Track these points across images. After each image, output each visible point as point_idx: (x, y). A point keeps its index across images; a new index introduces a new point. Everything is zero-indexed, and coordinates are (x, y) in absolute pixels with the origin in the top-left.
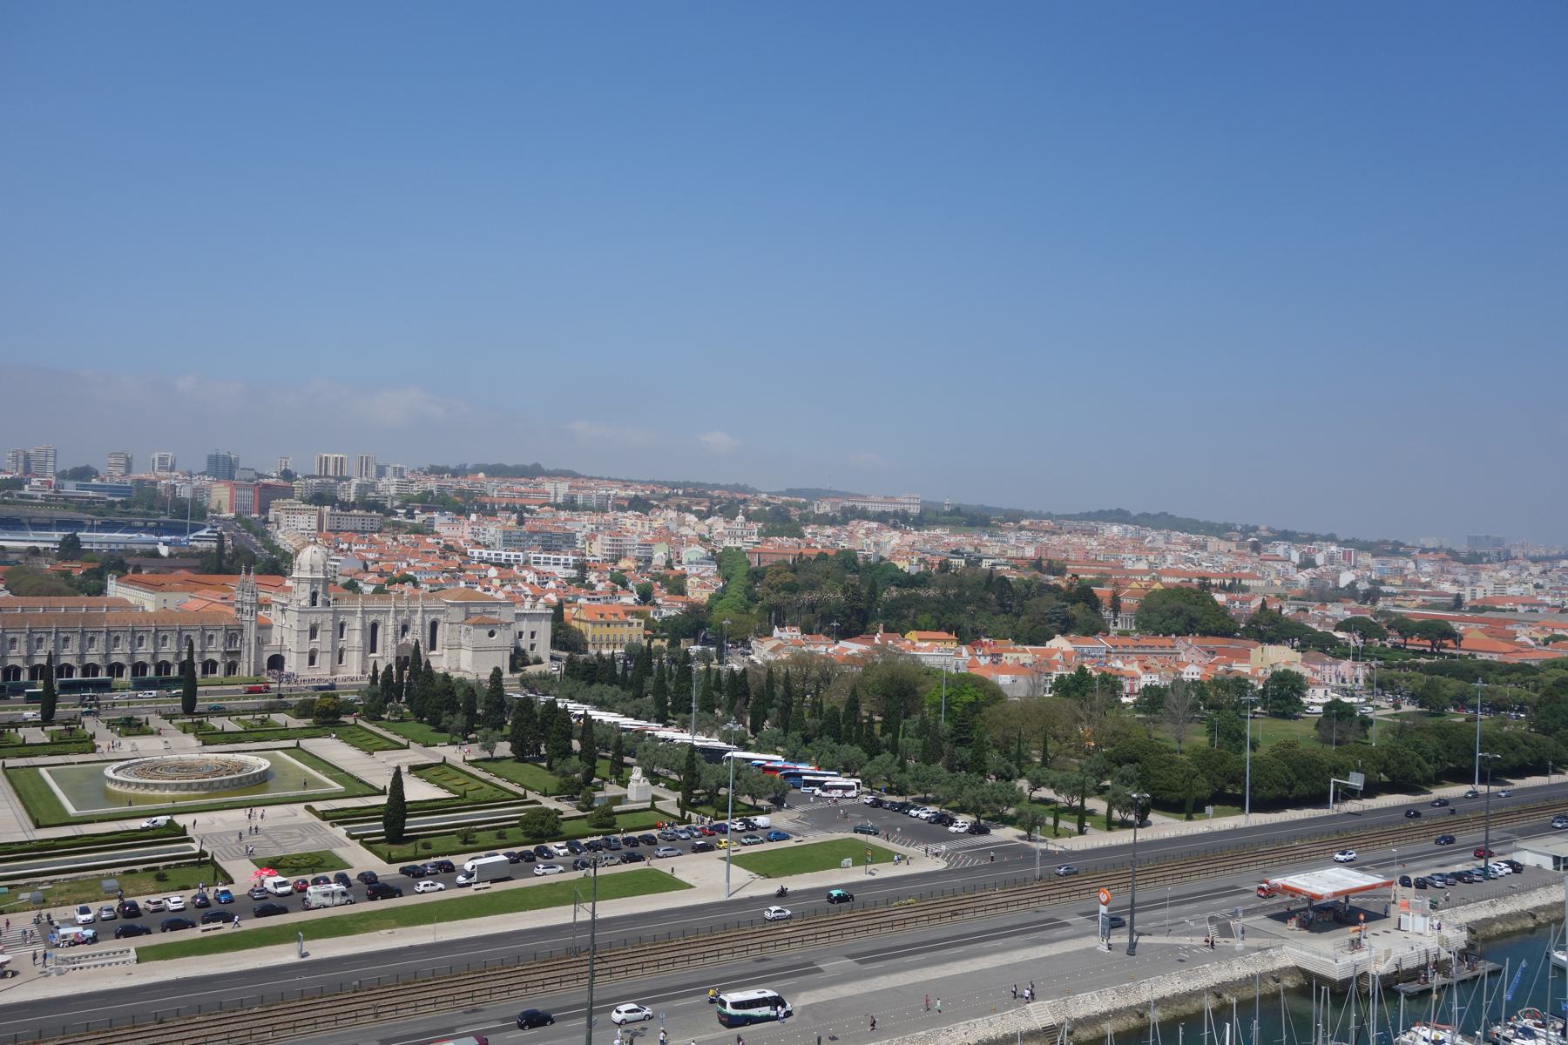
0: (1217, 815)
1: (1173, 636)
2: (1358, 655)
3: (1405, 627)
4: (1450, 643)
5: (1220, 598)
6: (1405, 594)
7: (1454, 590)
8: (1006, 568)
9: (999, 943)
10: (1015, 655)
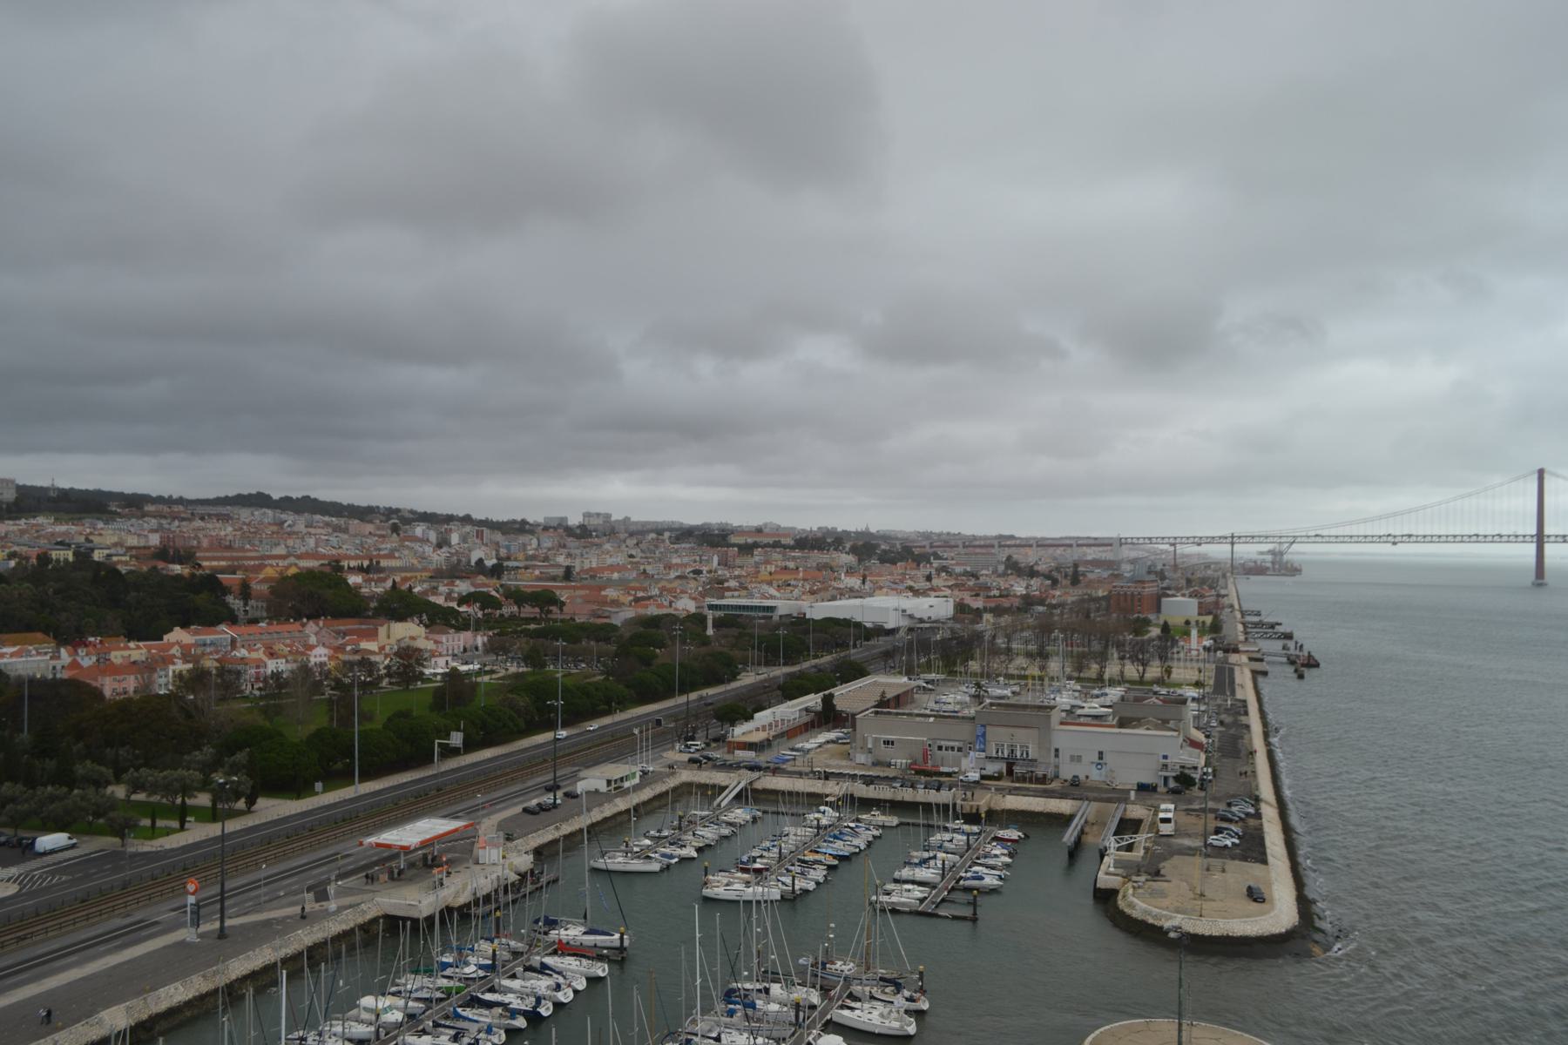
0: (325, 790)
1: (305, 620)
2: (478, 626)
3: (518, 597)
4: (553, 608)
5: (354, 579)
6: (526, 568)
7: (568, 562)
8: (123, 558)
9: (73, 958)
10: (126, 653)
